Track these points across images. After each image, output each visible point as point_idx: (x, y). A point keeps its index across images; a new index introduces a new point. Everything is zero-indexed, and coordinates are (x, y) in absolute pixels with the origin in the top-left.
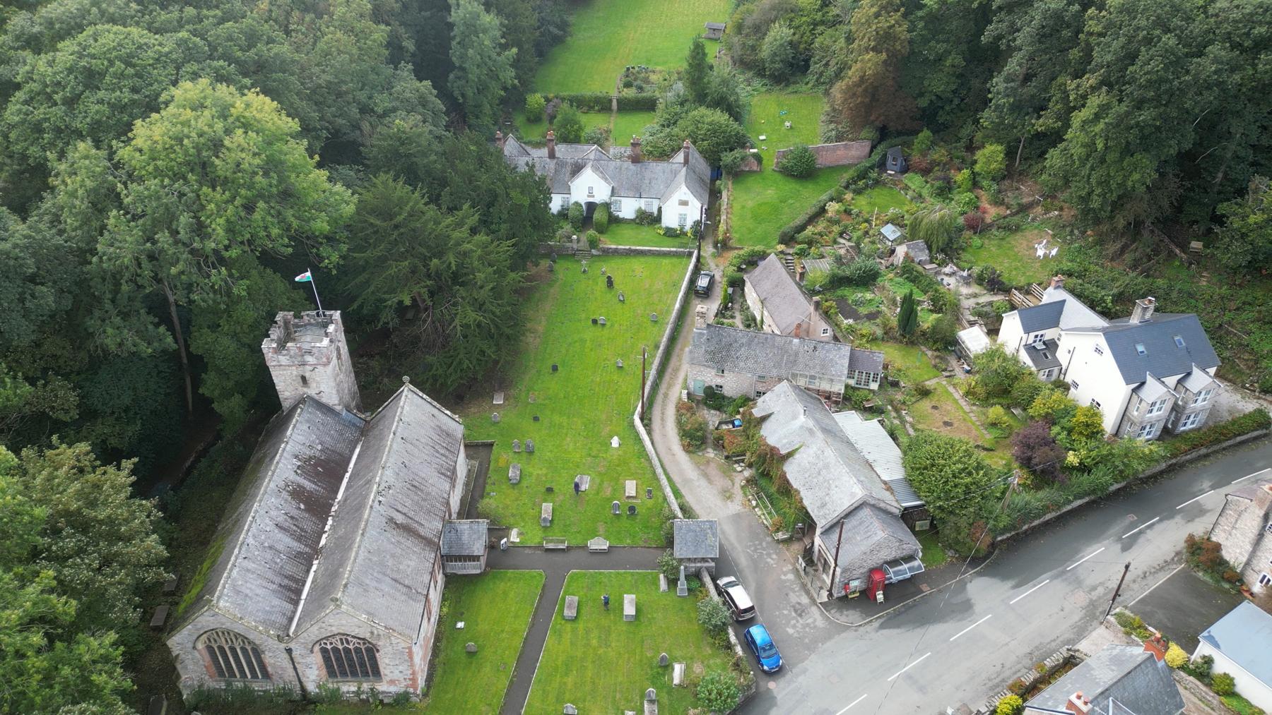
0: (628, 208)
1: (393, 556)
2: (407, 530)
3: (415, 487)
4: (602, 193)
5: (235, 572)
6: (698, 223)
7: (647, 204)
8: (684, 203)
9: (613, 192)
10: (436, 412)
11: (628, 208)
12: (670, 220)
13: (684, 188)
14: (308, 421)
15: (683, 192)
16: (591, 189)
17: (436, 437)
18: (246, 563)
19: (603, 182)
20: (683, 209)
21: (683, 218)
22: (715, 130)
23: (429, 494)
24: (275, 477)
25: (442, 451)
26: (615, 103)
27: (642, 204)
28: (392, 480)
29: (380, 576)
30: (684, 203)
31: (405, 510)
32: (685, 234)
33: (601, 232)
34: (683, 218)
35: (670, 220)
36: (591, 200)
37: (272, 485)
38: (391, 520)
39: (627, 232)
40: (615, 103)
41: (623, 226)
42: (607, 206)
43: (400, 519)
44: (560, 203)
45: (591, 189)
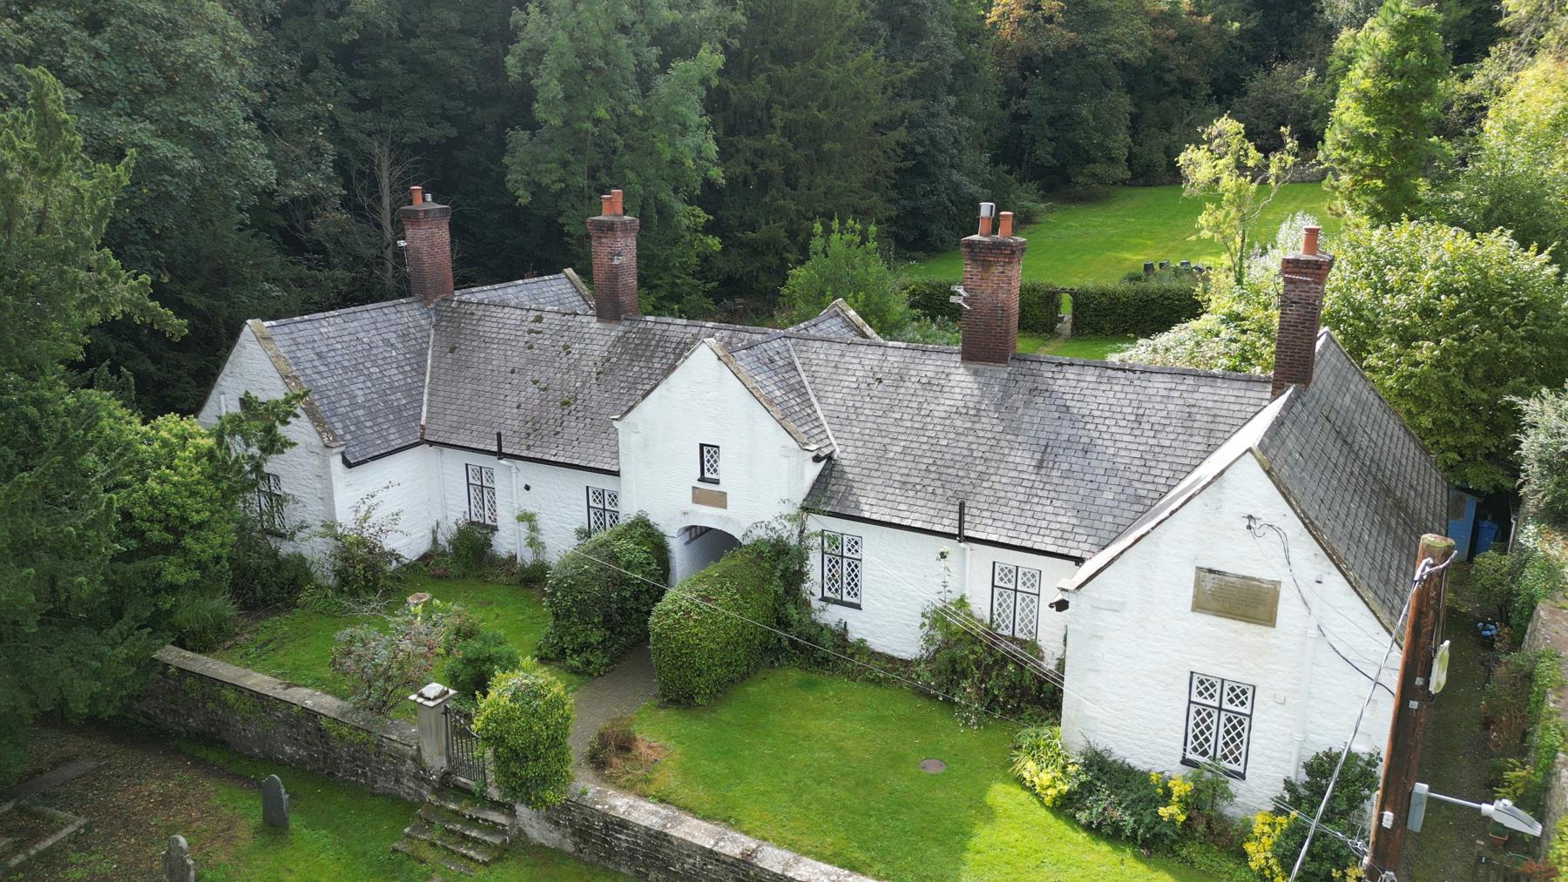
0: (893, 595)
4: (763, 491)
6: (1328, 782)
7: (1004, 584)
8: (1240, 601)
9: (828, 491)
11: (893, 595)
12: (1127, 692)
13: (1254, 490)
15: (1235, 508)
16: (708, 453)
19: (767, 425)
20: (1225, 648)
21: (1221, 712)
22: (1484, 299)
26: (1066, 310)
27: (971, 579)
30: (1240, 601)
32: (1228, 840)
33: (679, 699)
34: (1221, 712)
35: (1127, 692)
36: (708, 517)
39: (833, 723)
40: (1066, 310)
41: (835, 690)
42: (778, 564)
44: (578, 517)
45: (708, 453)
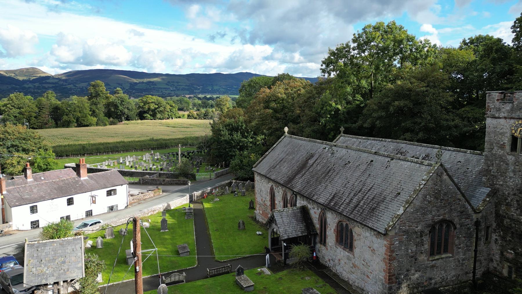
1: (293, 158)
2: (303, 166)
3: (328, 173)
5: (355, 140)
10: (404, 197)
14: (468, 161)
17: (371, 195)
18: (358, 143)
23: (320, 183)
24: (410, 146)
25: (355, 200)
28: (338, 155)
29: (287, 152)
31: (315, 165)
37: (403, 145)
38: (312, 156)
43: (311, 162)
